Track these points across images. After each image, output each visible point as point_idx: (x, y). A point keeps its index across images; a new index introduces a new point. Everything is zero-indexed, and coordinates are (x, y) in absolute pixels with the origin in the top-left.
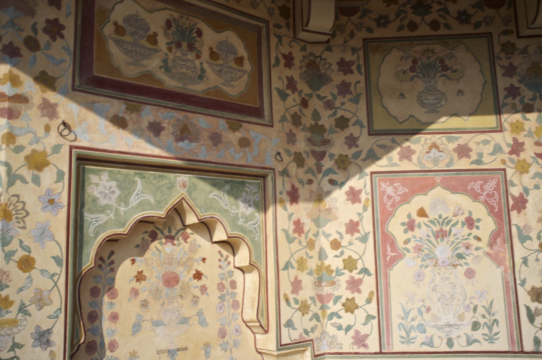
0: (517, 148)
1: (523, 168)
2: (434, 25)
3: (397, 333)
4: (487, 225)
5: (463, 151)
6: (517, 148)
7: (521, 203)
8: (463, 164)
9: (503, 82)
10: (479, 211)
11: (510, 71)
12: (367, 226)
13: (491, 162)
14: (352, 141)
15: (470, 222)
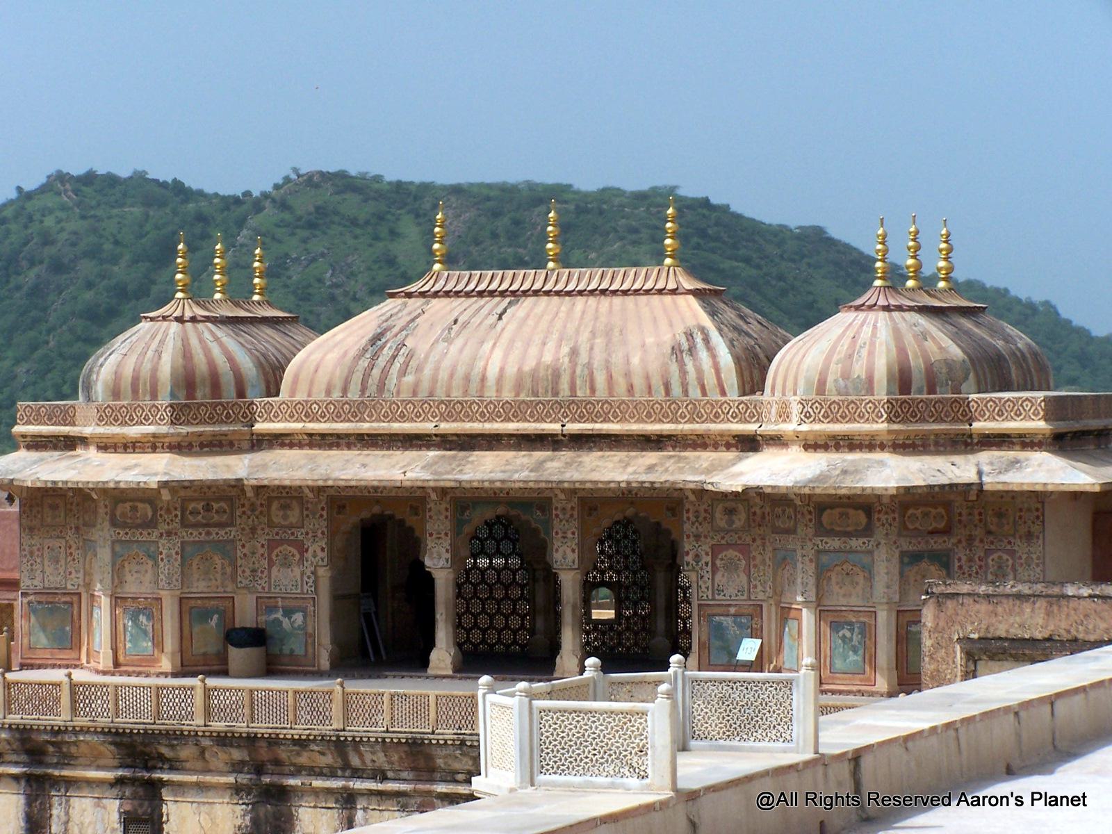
0: (307, 534)
1: (308, 540)
2: (287, 493)
3: (273, 587)
4: (298, 557)
5: (293, 534)
6: (307, 534)
7: (307, 551)
8: (292, 538)
9: (305, 513)
10: (295, 552)
11: (307, 509)
12: (266, 555)
13: (300, 538)
14: (263, 529)
15: (293, 555)
